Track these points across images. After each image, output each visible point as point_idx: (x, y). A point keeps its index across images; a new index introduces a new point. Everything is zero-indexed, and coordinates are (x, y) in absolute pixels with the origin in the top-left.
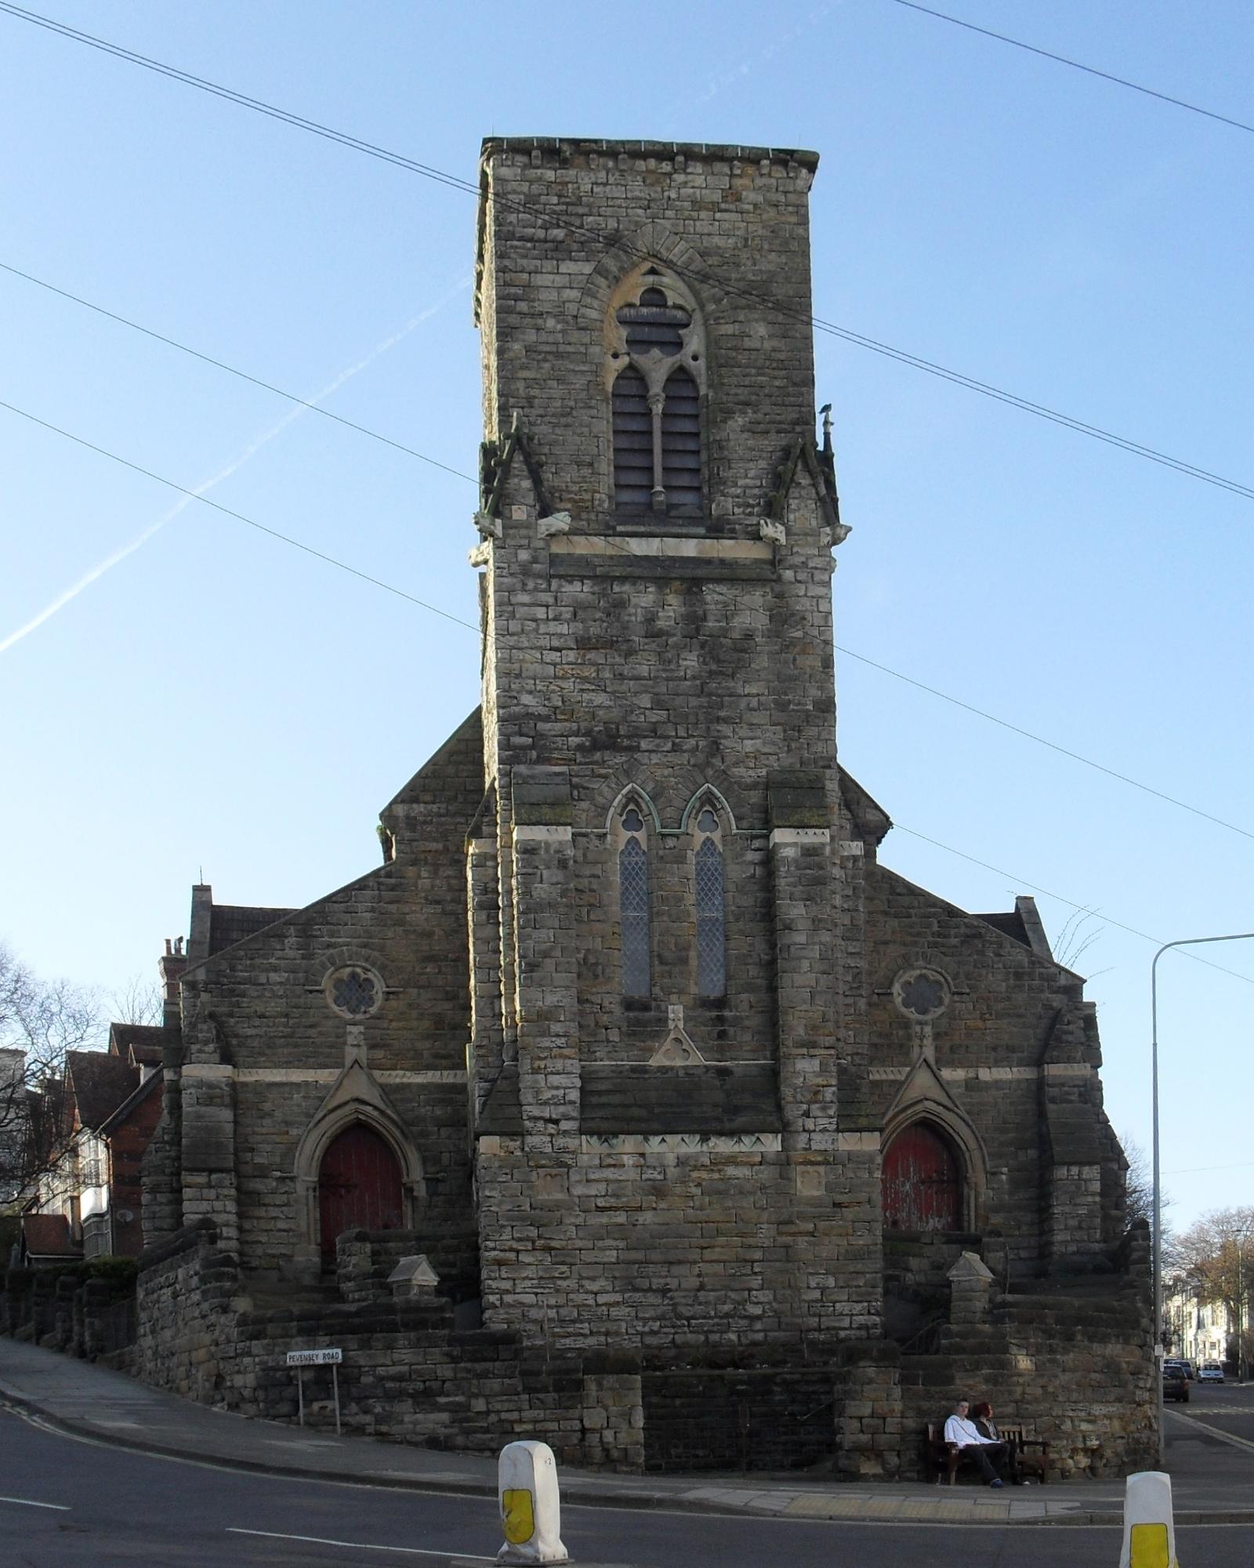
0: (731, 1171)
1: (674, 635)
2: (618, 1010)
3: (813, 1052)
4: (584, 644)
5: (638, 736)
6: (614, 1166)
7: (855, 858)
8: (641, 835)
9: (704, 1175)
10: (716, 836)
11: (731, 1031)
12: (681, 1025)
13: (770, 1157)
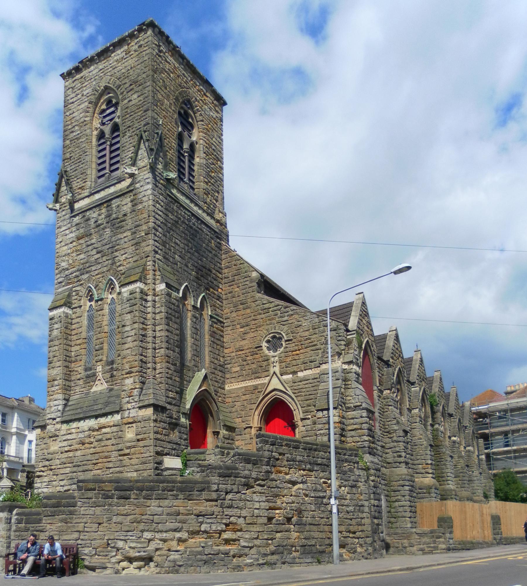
1: (103, 224)
2: (83, 372)
3: (132, 375)
4: (79, 238)
5: (92, 266)
7: (161, 290)
8: (93, 303)
11: (115, 373)
12: (100, 374)
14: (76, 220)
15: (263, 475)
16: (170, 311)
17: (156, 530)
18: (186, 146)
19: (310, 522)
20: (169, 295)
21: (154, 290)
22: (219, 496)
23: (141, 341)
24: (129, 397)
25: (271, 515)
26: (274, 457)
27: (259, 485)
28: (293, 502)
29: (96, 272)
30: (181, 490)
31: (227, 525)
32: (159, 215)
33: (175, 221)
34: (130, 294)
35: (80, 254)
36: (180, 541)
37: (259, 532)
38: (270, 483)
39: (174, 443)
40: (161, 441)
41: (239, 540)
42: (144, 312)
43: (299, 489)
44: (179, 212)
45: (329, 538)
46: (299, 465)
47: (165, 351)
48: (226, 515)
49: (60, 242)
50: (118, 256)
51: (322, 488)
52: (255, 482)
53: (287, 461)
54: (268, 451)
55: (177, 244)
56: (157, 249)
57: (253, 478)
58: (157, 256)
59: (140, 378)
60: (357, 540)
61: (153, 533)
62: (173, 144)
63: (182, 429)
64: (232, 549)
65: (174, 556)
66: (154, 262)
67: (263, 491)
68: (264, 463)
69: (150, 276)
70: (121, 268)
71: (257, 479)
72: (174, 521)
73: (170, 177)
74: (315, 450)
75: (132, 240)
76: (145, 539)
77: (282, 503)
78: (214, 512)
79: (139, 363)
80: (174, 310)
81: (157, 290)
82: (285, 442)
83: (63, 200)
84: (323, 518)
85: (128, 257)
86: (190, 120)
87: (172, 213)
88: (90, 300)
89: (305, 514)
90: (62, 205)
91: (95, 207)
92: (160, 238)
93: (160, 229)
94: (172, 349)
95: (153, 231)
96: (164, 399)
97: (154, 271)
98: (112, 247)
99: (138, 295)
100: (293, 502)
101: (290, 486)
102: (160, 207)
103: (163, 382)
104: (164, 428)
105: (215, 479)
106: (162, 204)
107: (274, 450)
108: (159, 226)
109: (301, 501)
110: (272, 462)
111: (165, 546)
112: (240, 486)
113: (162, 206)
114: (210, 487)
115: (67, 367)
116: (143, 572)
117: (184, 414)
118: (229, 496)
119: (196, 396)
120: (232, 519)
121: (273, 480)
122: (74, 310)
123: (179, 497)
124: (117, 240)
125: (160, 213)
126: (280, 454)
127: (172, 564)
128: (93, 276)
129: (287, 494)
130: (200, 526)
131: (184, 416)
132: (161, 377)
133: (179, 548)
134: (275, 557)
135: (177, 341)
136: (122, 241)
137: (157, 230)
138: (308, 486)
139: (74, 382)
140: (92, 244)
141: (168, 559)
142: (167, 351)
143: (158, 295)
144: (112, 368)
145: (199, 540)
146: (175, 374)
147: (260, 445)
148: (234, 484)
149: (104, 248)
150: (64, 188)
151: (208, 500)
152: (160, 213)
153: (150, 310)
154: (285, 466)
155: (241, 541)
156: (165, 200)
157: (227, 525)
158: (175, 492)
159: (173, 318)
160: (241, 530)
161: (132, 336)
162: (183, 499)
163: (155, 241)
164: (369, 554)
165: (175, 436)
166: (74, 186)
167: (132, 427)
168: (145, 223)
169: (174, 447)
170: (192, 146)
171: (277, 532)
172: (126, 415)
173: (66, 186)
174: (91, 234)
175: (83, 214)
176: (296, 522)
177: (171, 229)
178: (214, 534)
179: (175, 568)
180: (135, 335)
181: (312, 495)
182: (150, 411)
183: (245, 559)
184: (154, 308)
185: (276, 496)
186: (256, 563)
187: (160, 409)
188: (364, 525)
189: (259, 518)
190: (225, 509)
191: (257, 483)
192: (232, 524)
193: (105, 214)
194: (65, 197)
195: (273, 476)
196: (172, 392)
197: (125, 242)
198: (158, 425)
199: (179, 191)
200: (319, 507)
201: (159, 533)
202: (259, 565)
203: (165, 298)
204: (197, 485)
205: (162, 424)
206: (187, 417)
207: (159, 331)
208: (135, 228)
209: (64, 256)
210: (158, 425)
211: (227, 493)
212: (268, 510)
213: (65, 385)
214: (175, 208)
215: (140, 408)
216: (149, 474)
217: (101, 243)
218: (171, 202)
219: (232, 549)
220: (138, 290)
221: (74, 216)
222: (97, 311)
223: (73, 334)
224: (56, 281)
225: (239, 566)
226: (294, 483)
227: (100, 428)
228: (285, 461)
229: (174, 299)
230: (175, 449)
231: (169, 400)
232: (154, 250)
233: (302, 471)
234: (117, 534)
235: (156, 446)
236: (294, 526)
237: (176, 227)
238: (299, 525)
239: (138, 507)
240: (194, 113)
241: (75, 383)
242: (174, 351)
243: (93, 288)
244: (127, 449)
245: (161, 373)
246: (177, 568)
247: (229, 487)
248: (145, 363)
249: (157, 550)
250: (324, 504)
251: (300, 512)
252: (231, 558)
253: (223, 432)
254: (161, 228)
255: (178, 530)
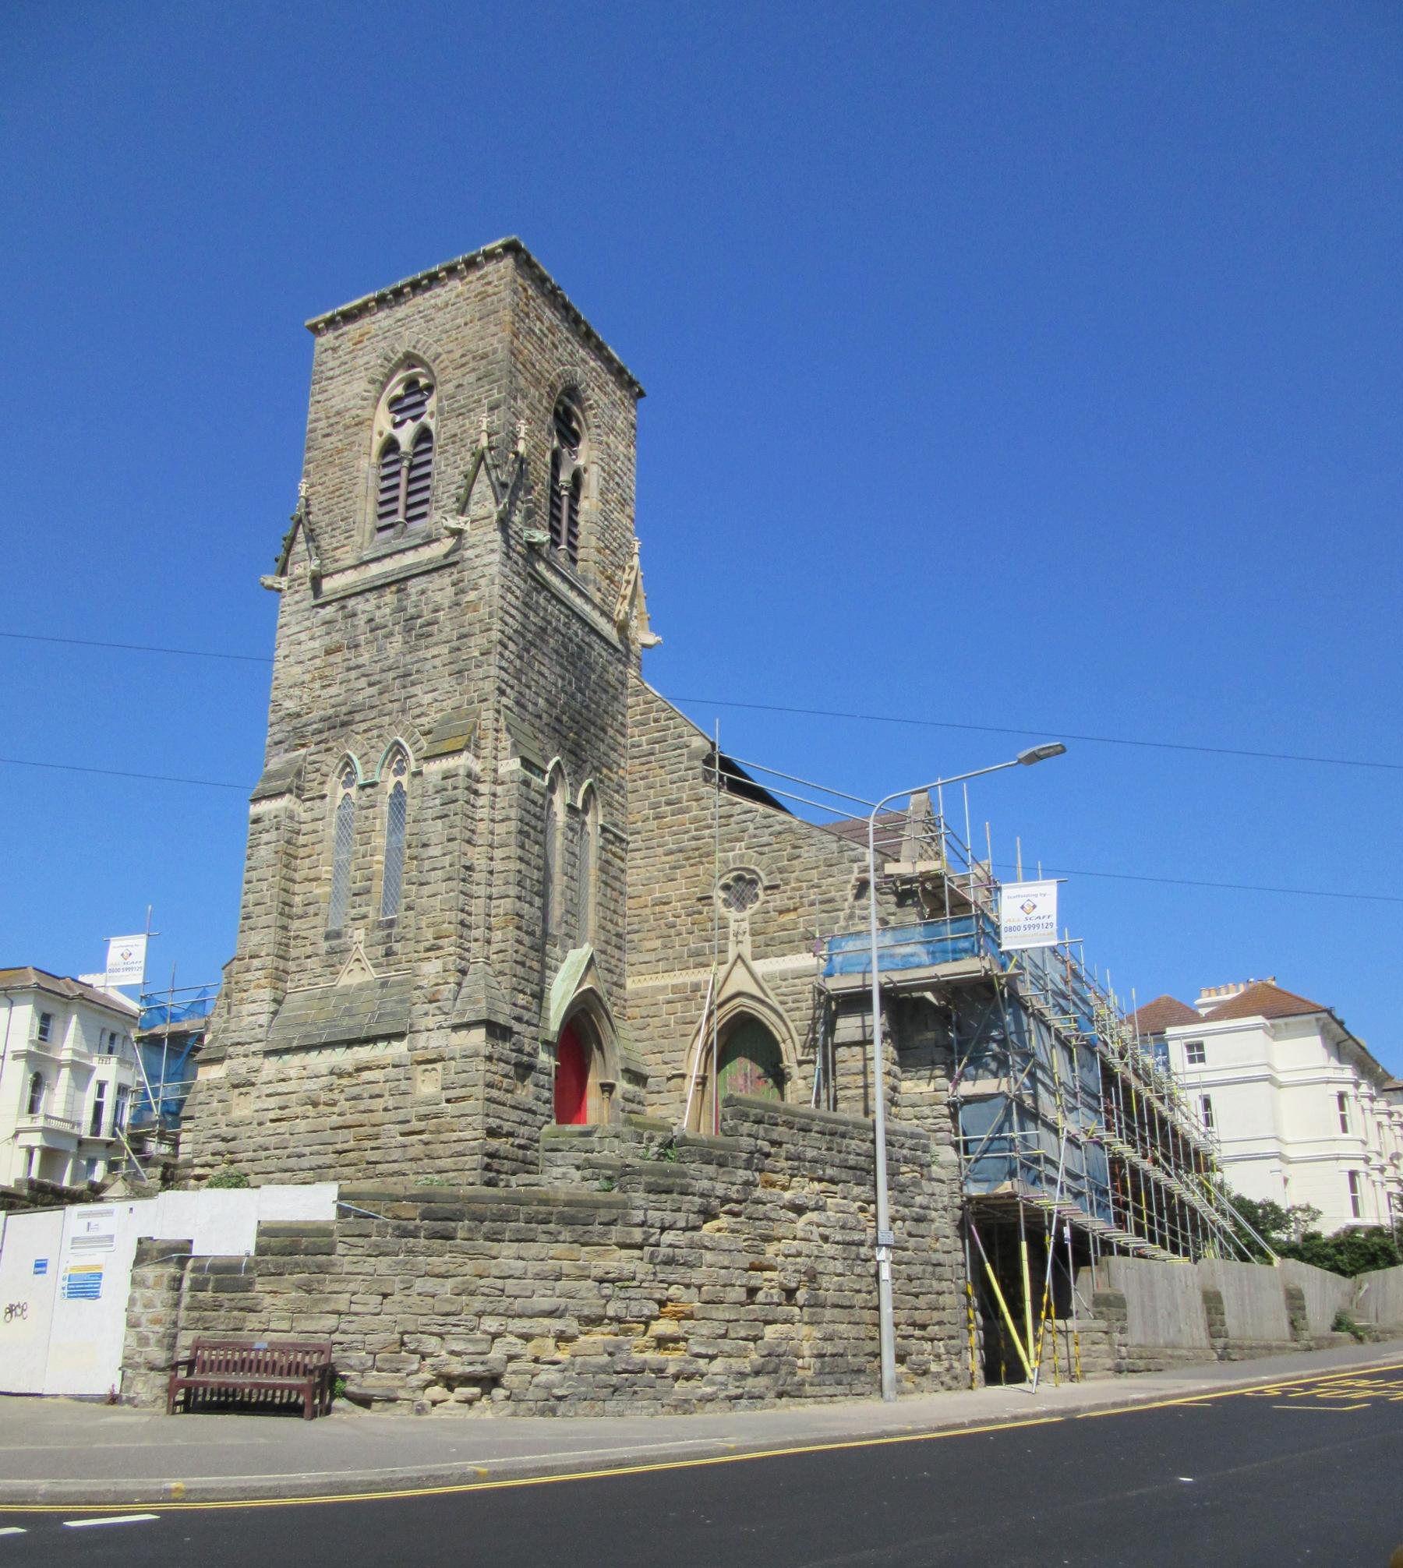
0: (366, 1075)
1: (386, 626)
4: (329, 652)
6: (283, 1080)
7: (512, 772)
8: (353, 791)
9: (345, 1081)
10: (404, 779)
11: (397, 947)
12: (361, 947)
13: (397, 1061)
14: (329, 612)
15: (738, 1191)
16: (528, 818)
17: (510, 1313)
18: (565, 477)
19: (836, 1300)
20: (526, 783)
21: (495, 771)
22: (647, 1236)
23: (464, 880)
24: (431, 1002)
25: (753, 1283)
26: (760, 1151)
27: (730, 1213)
28: (799, 1254)
29: (364, 726)
30: (568, 1221)
31: (662, 1303)
32: (512, 616)
33: (540, 627)
34: (444, 778)
35: (329, 685)
36: (562, 1338)
37: (728, 1321)
38: (752, 1209)
39: (524, 1110)
40: (499, 1103)
41: (686, 1340)
42: (472, 818)
43: (810, 1223)
44: (550, 608)
45: (872, 1339)
46: (812, 1170)
47: (514, 904)
48: (662, 1281)
49: (286, 657)
50: (416, 695)
51: (858, 1221)
52: (722, 1206)
53: (787, 1159)
54: (749, 1135)
55: (543, 675)
56: (504, 686)
57: (718, 1197)
58: (504, 700)
59: (458, 960)
60: (927, 1346)
61: (502, 1320)
62: (542, 474)
63: (542, 1077)
64: (673, 1361)
65: (548, 1375)
66: (498, 711)
67: (738, 1227)
68: (741, 1163)
69: (488, 743)
70: (424, 720)
71: (725, 1200)
72: (549, 1292)
73: (535, 540)
74: (843, 1136)
75: (451, 663)
76: (485, 1332)
77: (777, 1255)
78: (635, 1273)
79: (456, 929)
80: (534, 815)
81: (501, 771)
82: (784, 1118)
83: (298, 570)
84: (859, 1291)
85: (440, 698)
86: (574, 425)
87: (535, 612)
88: (347, 784)
89: (824, 1281)
90: (294, 580)
91: (370, 590)
92: (511, 662)
93: (511, 646)
94: (528, 899)
95: (499, 648)
96: (507, 1009)
97: (497, 731)
98: (405, 676)
99: (462, 782)
100: (799, 1254)
101: (792, 1215)
102: (514, 599)
103: (507, 971)
104: (506, 1076)
105: (639, 1197)
106: (518, 593)
107: (762, 1133)
108: (510, 638)
109: (816, 1253)
110: (756, 1160)
111: (530, 1350)
112: (691, 1215)
113: (517, 598)
114: (628, 1214)
115: (285, 928)
116: (472, 1414)
117: (546, 1043)
118: (669, 1237)
119: (573, 1005)
120: (673, 1291)
121: (758, 1202)
122: (308, 804)
123: (561, 1238)
124: (416, 662)
125: (514, 612)
126: (773, 1143)
127: (543, 1394)
128: (357, 733)
129: (786, 1235)
130: (605, 1306)
131: (545, 1047)
132: (503, 961)
133: (558, 1356)
134: (763, 1381)
135: (538, 881)
136: (428, 665)
137: (506, 647)
138: (828, 1217)
139: (298, 962)
140: (358, 667)
141: (536, 1380)
142: (518, 904)
143: (503, 783)
144: (389, 936)
145: (599, 1337)
146: (533, 954)
147: (731, 1123)
148: (679, 1210)
149: (384, 675)
150: (300, 547)
151: (623, 1246)
152: (514, 612)
153: (481, 813)
154: (782, 1170)
155: (691, 1341)
156: (523, 586)
157: (662, 1303)
158: (552, 1225)
159: (532, 832)
160: (690, 1317)
161: (443, 868)
162: (571, 1243)
163: (502, 668)
164: (955, 1378)
165: (525, 1093)
166: (323, 543)
167: (434, 1069)
168: (482, 632)
169: (525, 1118)
170: (577, 478)
171: (767, 1323)
172: (421, 1044)
173: (307, 542)
174: (356, 646)
175: (343, 603)
176: (806, 1300)
177: (532, 644)
178: (635, 1325)
179: (551, 1404)
180: (451, 865)
181: (839, 1238)
182: (479, 1036)
183: (700, 1384)
184: (493, 808)
185: (767, 1239)
186: (722, 1395)
187: (498, 1031)
188: (944, 1309)
189: (728, 1289)
190: (658, 1267)
191: (727, 1207)
192: (671, 1301)
193: (392, 606)
194: (302, 564)
195: (759, 1192)
196: (525, 993)
197: (435, 667)
198: (494, 1068)
199: (551, 566)
200: (851, 1268)
201: (516, 1320)
202: (730, 1398)
203: (518, 789)
204: (602, 1211)
205: (502, 1064)
206: (551, 1049)
207: (503, 859)
208: (458, 639)
209: (291, 687)
210: (494, 1068)
211: (663, 1229)
212: (746, 1270)
213: (277, 969)
214: (542, 601)
215: (456, 1028)
216: (471, 1180)
217: (380, 664)
218: (535, 589)
219: (673, 1361)
220: (462, 772)
221: (323, 606)
222: (362, 808)
223: (301, 855)
224: (268, 740)
225: (686, 1401)
226: (800, 1210)
227: (359, 1070)
228: (782, 1160)
229: (536, 791)
230: (525, 1123)
231: (518, 1011)
232: (499, 689)
233: (816, 1183)
234: (424, 1320)
235: (487, 1115)
236: (801, 1308)
237: (543, 640)
238: (812, 1306)
239: (471, 1259)
240: (583, 412)
241: (299, 965)
242: (531, 904)
243: (354, 758)
244: (420, 1120)
245: (501, 951)
246: (552, 1402)
247: (668, 1217)
248: (469, 927)
249: (511, 1358)
250: (863, 1260)
251: (812, 1276)
252: (670, 1381)
253: (623, 1086)
254: (513, 641)
255: (558, 1313)
